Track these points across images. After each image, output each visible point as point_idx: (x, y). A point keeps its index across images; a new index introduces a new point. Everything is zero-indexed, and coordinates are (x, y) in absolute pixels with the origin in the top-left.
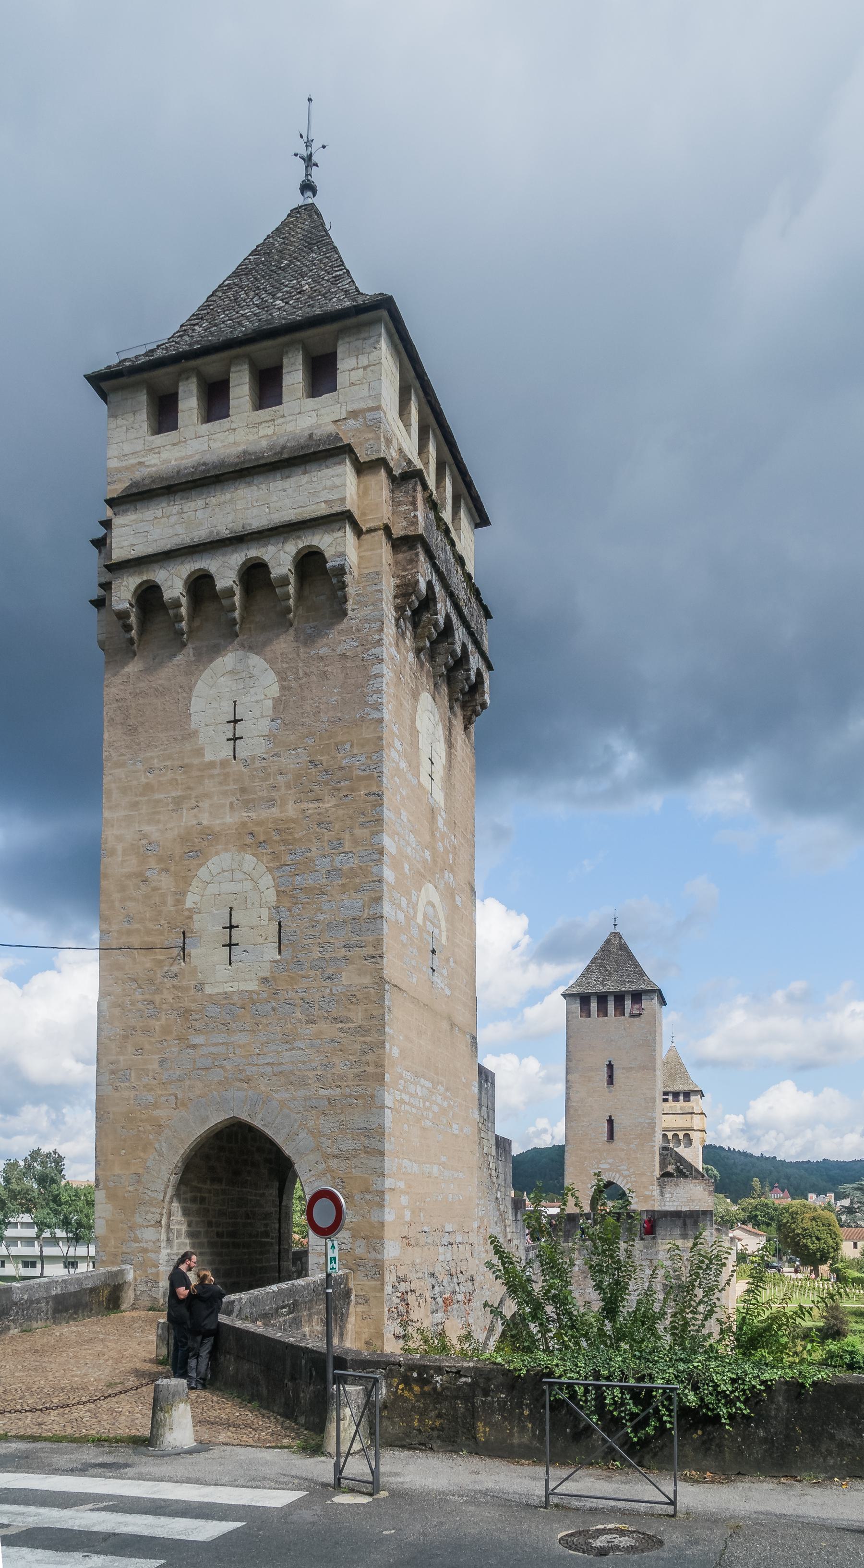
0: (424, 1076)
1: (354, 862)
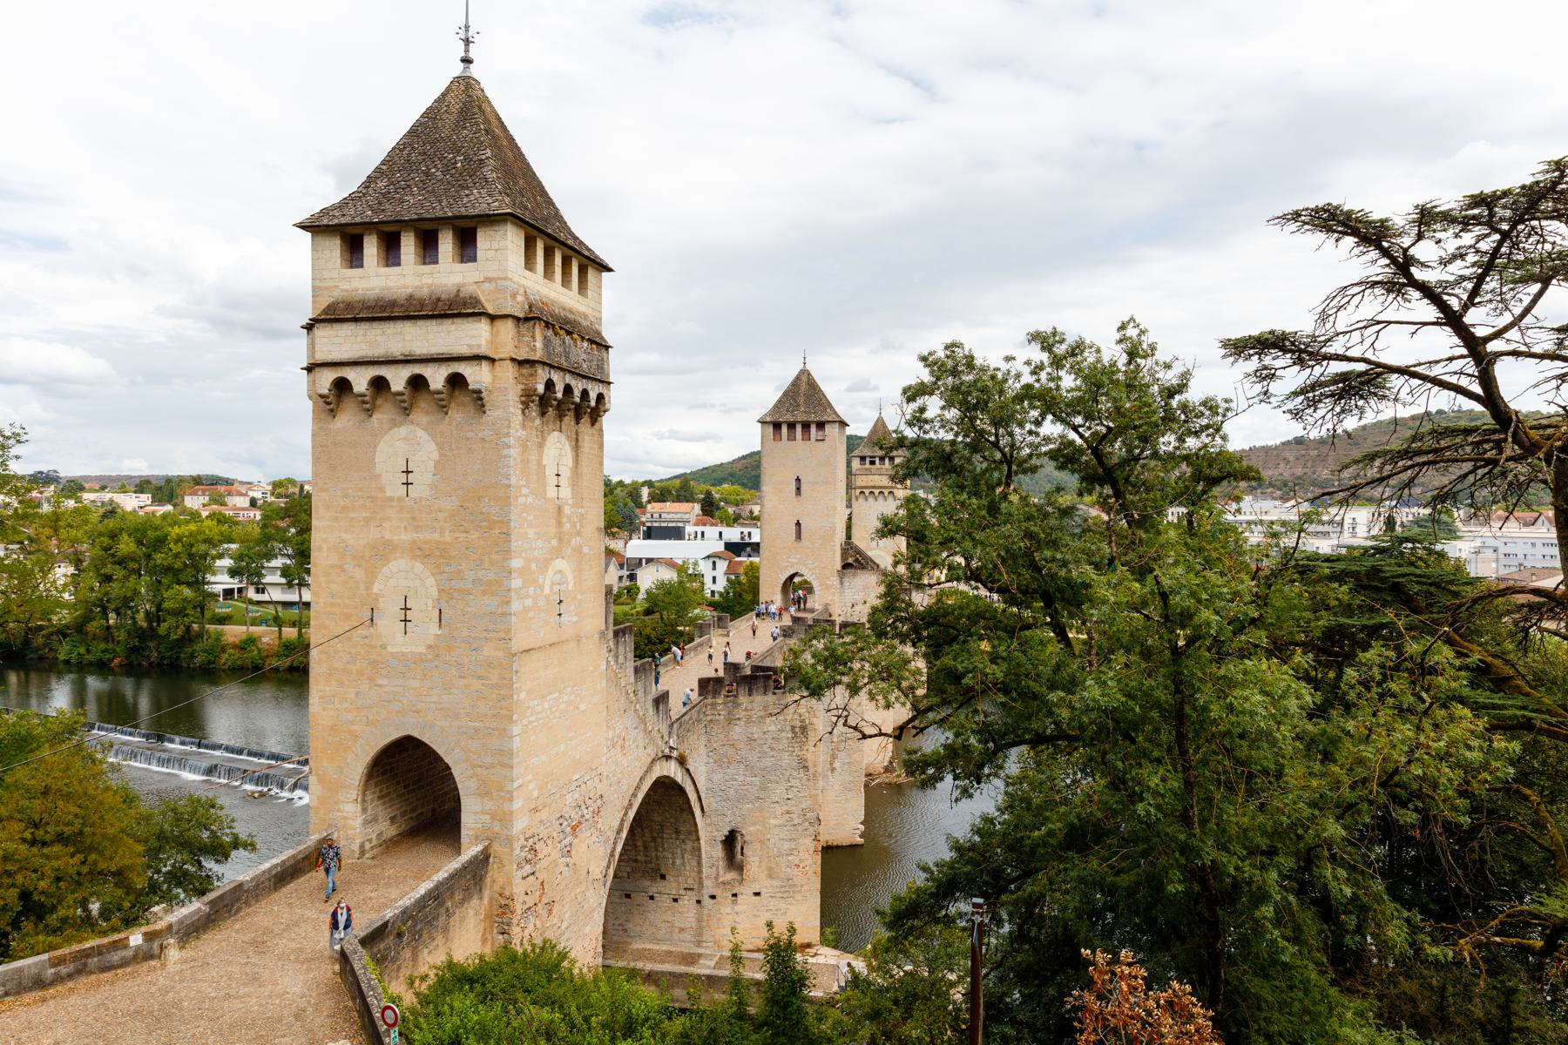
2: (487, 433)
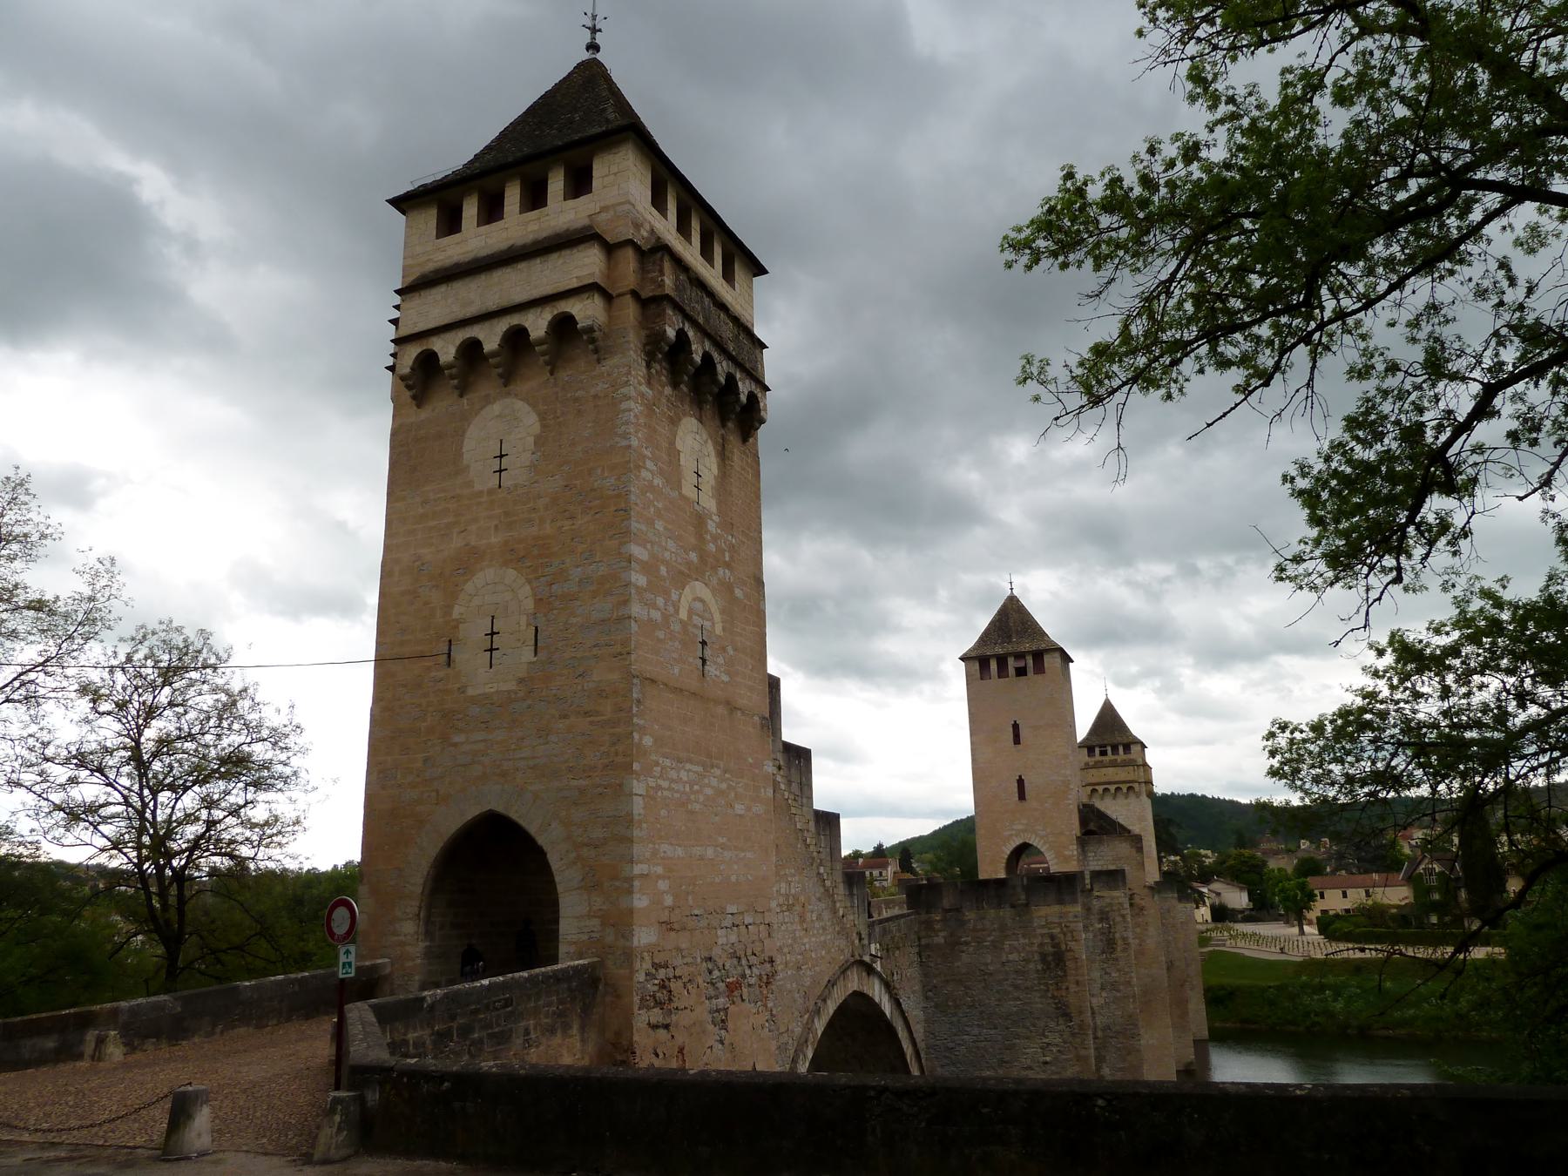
0: (690, 761)
2: (601, 387)
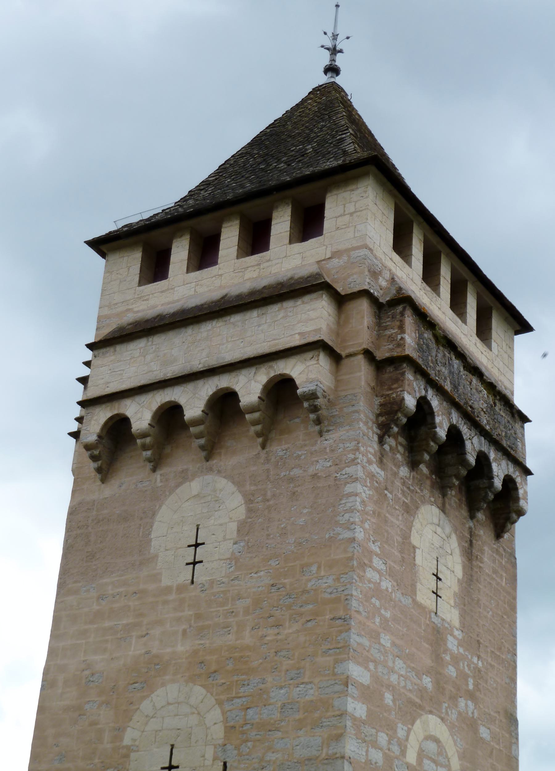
1: (312, 694)
2: (321, 465)
